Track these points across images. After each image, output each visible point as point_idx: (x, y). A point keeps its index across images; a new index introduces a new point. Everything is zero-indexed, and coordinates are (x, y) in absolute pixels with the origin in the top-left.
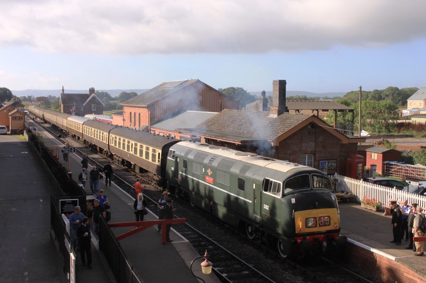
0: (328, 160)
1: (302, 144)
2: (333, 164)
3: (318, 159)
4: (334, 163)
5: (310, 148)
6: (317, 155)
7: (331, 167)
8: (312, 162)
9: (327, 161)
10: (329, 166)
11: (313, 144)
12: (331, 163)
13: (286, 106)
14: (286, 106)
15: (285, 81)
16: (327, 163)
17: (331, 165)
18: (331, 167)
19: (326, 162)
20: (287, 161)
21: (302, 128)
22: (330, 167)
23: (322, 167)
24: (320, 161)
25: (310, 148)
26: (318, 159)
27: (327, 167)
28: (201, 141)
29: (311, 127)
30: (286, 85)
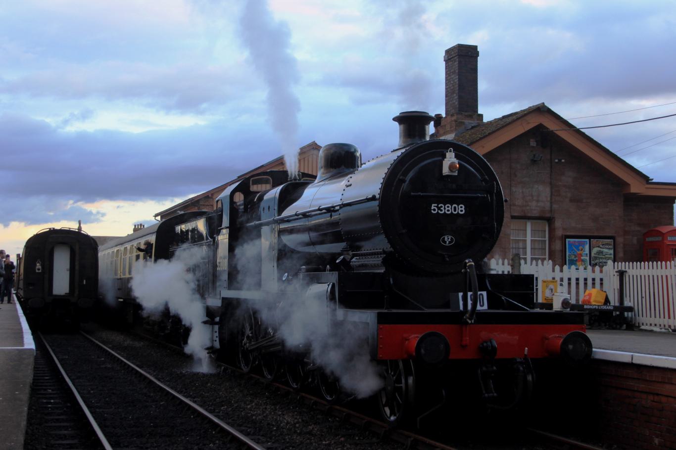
0: (590, 238)
1: (514, 189)
2: (605, 250)
3: (559, 233)
4: (609, 249)
5: (538, 201)
6: (558, 224)
7: (599, 258)
8: (545, 241)
9: (588, 240)
10: (593, 255)
11: (544, 191)
12: (599, 247)
13: (479, 112)
14: (479, 112)
15: (475, 48)
16: (587, 247)
17: (600, 253)
18: (599, 258)
19: (583, 244)
20: (429, 128)
21: (514, 139)
22: (596, 258)
23: (573, 257)
24: (567, 240)
25: (538, 201)
26: (559, 233)
27: (588, 258)
28: (262, 218)
29: (537, 145)
30: (478, 58)
